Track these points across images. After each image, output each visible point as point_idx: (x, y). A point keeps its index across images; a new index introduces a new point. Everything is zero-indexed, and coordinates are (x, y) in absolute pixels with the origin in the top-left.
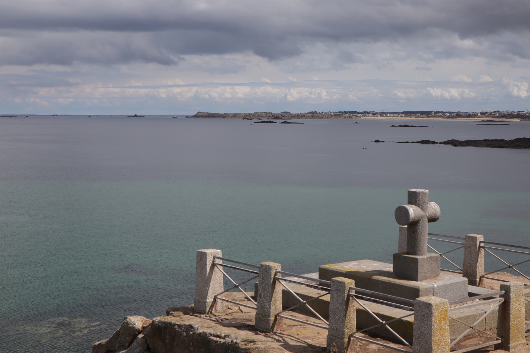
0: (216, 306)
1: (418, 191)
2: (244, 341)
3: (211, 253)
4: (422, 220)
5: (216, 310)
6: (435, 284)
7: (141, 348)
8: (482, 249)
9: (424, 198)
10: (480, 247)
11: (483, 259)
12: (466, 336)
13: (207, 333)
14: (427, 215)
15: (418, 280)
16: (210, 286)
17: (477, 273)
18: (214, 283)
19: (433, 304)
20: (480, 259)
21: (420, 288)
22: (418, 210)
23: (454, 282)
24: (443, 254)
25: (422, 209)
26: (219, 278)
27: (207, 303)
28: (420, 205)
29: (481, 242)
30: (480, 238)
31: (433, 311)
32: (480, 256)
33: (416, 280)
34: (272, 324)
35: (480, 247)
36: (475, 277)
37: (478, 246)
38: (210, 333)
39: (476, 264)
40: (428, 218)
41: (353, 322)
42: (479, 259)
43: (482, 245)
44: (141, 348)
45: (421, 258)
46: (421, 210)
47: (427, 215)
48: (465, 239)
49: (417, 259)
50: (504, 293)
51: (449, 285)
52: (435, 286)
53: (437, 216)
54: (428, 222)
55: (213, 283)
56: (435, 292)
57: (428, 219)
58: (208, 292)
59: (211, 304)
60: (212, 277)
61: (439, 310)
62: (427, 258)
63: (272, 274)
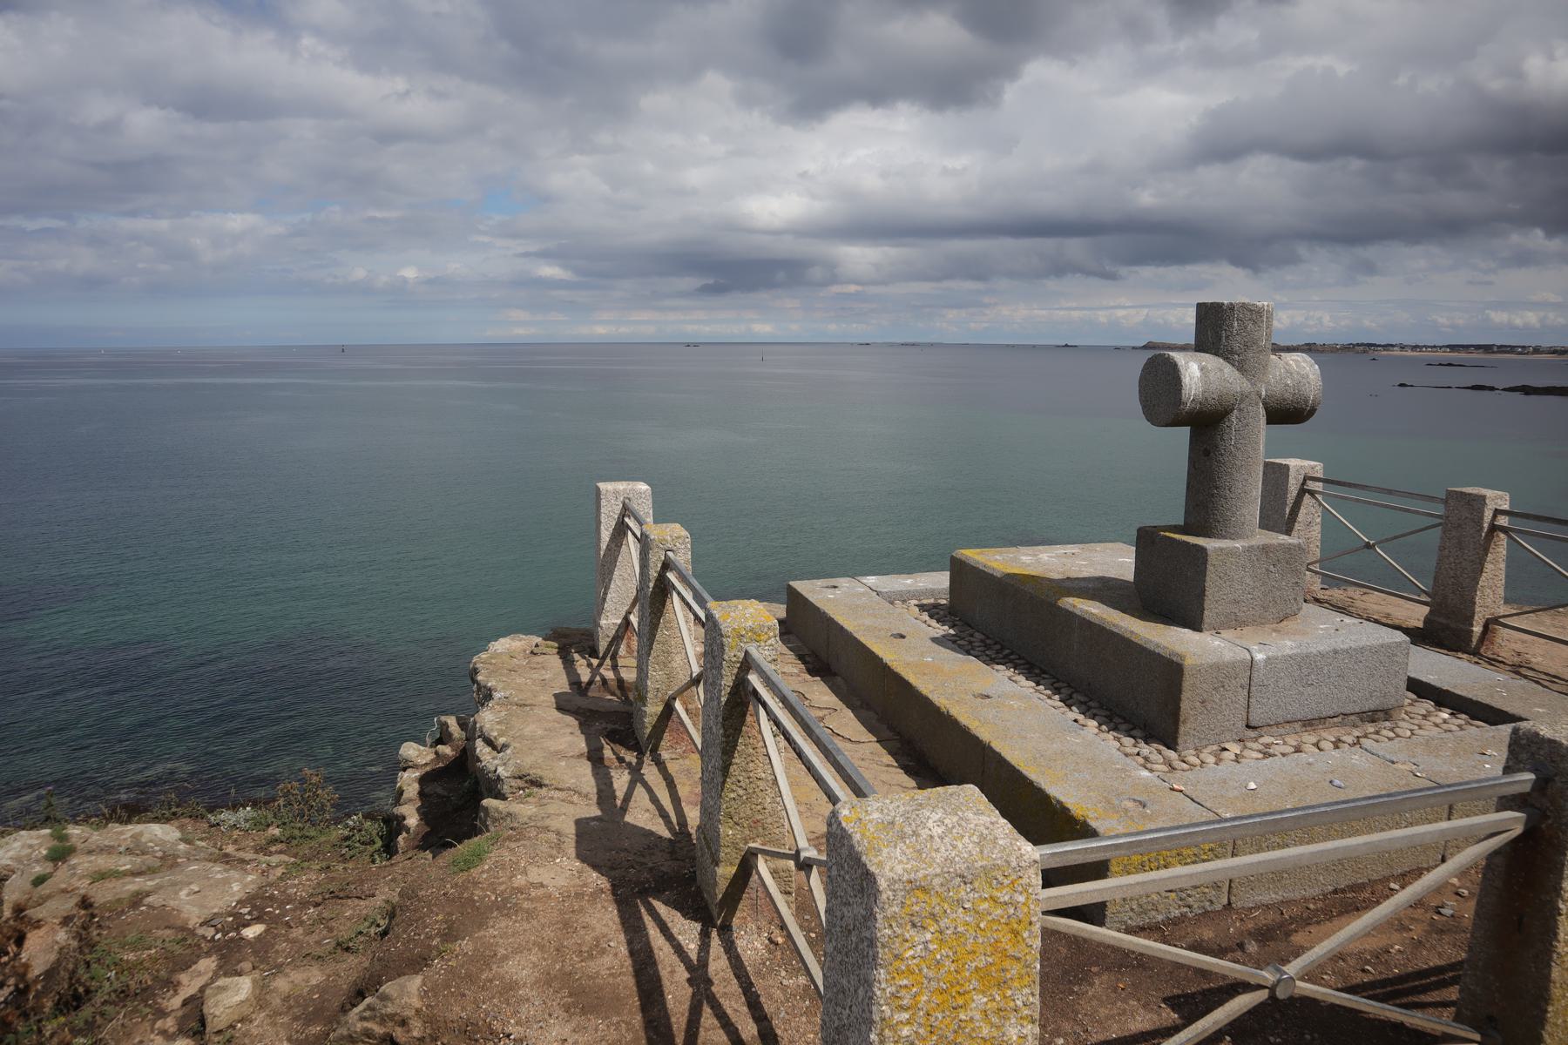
2: (520, 778)
3: (616, 492)
4: (1240, 410)
6: (1260, 651)
8: (1502, 536)
9: (1250, 326)
10: (1494, 528)
11: (1503, 566)
12: (1343, 891)
14: (1264, 393)
15: (1205, 626)
16: (612, 582)
17: (1477, 609)
19: (882, 883)
21: (1188, 662)
23: (1346, 646)
24: (1379, 543)
25: (1241, 368)
27: (601, 628)
28: (1232, 352)
29: (1497, 512)
30: (1497, 499)
31: (883, 932)
32: (1490, 557)
33: (1195, 624)
34: (654, 727)
35: (1494, 528)
36: (1469, 619)
37: (1486, 525)
39: (1476, 581)
40: (1265, 404)
41: (769, 800)
42: (1488, 567)
43: (1503, 521)
45: (1221, 549)
47: (1264, 393)
48: (1445, 502)
49: (1202, 551)
50: (1527, 788)
51: (1322, 655)
52: (1259, 657)
53: (1306, 401)
54: (1269, 422)
56: (1255, 680)
57: (1266, 409)
58: (604, 599)
59: (614, 632)
60: (620, 558)
61: (944, 922)
62: (1250, 549)
63: (652, 565)
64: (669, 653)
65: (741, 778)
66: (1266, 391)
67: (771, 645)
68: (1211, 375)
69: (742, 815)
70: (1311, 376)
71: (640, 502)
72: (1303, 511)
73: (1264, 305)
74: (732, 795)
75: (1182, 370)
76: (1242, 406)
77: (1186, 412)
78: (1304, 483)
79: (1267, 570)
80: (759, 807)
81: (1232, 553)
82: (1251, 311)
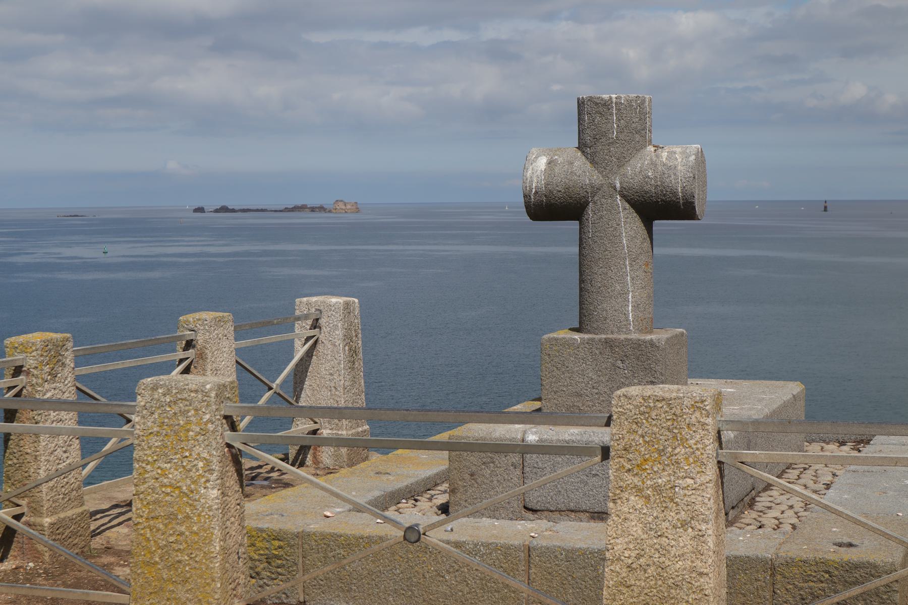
4: (595, 203)
14: (618, 185)
16: (303, 392)
18: (315, 386)
25: (593, 162)
26: (331, 374)
40: (623, 196)
41: (32, 470)
46: (588, 165)
47: (618, 185)
53: (675, 194)
55: (311, 386)
57: (628, 202)
60: (310, 369)
62: (590, 342)
65: (15, 451)
66: (621, 183)
67: (34, 356)
68: (557, 170)
69: (16, 478)
70: (679, 168)
71: (330, 314)
73: (611, 98)
74: (10, 462)
76: (596, 198)
77: (534, 205)
79: (614, 365)
80: (26, 475)
82: (597, 104)
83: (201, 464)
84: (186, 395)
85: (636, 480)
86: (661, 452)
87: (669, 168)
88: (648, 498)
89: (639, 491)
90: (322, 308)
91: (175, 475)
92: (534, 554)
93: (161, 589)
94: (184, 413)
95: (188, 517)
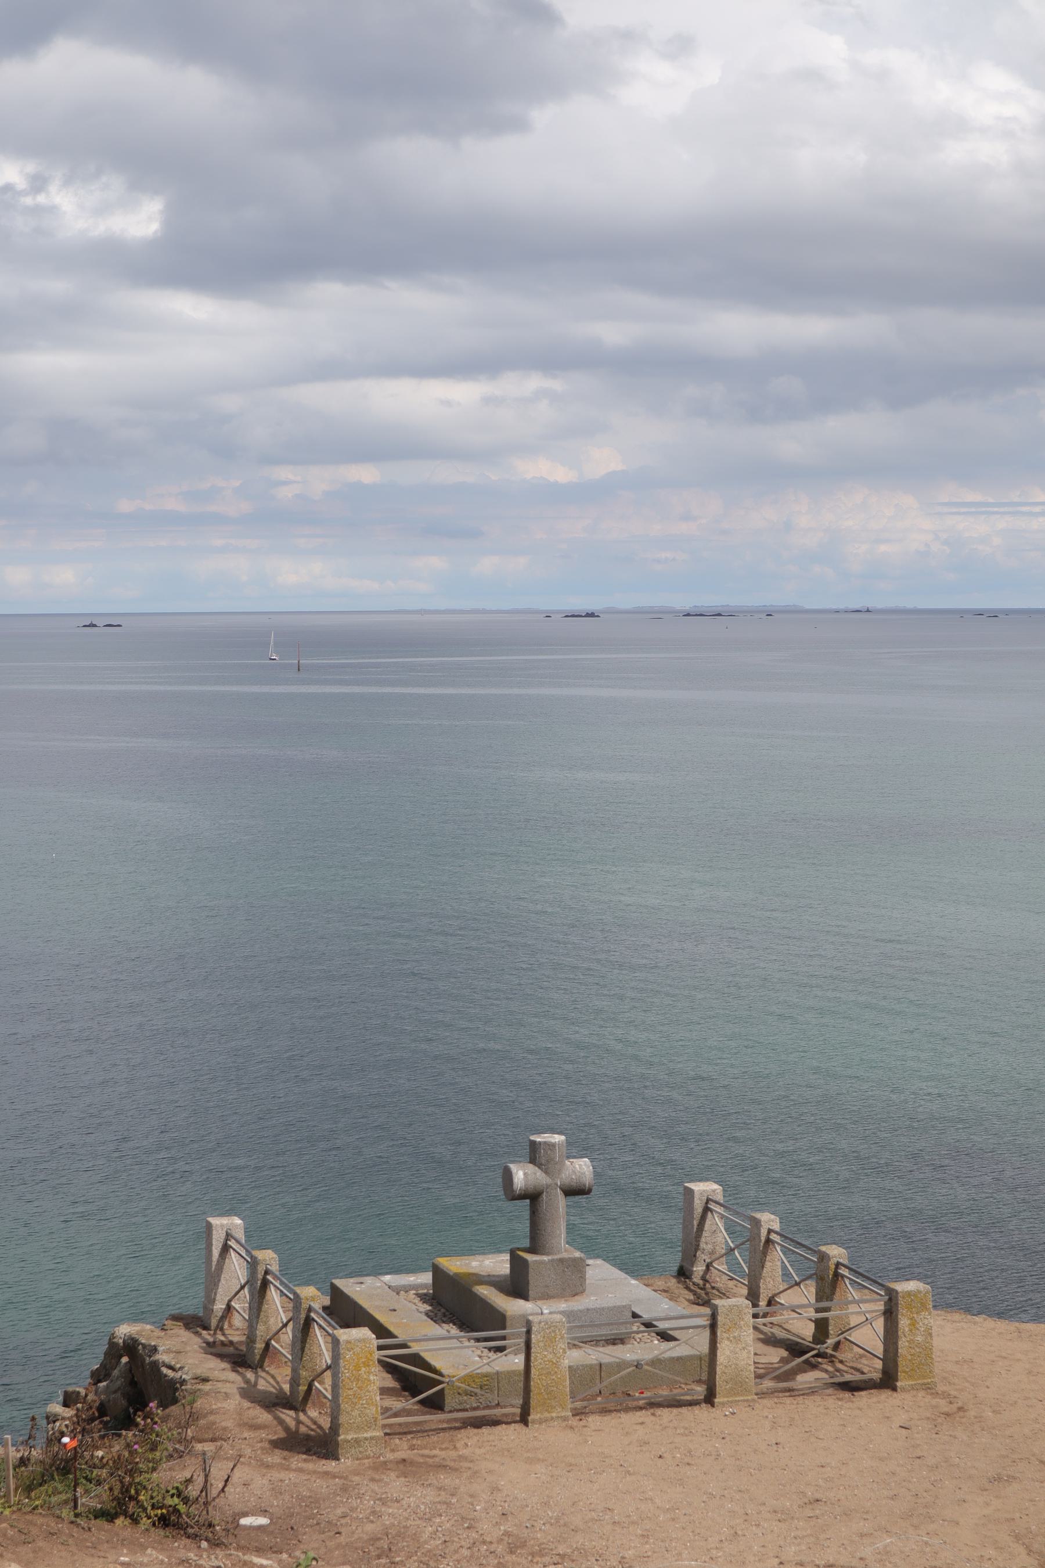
0: (230, 1318)
1: (538, 1140)
2: (196, 1379)
3: (222, 1226)
4: (547, 1192)
5: (231, 1326)
6: (546, 1309)
7: (123, 1380)
13: (161, 1361)
14: (559, 1184)
15: (530, 1299)
17: (762, 1291)
18: (228, 1278)
19: (341, 1341)
20: (771, 1264)
21: (508, 1314)
22: (535, 1174)
25: (546, 1172)
28: (541, 1164)
32: (768, 1258)
35: (768, 1241)
38: (163, 1362)
40: (561, 1189)
44: (123, 1380)
45: (536, 1261)
46: (544, 1174)
47: (559, 1184)
51: (581, 1311)
53: (585, 1186)
57: (563, 1191)
60: (225, 1267)
62: (552, 1260)
63: (259, 1272)
64: (268, 1317)
70: (587, 1173)
72: (708, 1222)
75: (514, 1175)
78: (707, 1203)
81: (542, 1262)
83: (561, 1351)
84: (554, 1324)
85: (728, 1335)
86: (735, 1324)
87: (582, 1174)
88: (731, 1341)
89: (728, 1339)
90: (231, 1227)
91: (550, 1356)
92: (603, 1366)
93: (545, 1403)
94: (554, 1331)
95: (556, 1372)
